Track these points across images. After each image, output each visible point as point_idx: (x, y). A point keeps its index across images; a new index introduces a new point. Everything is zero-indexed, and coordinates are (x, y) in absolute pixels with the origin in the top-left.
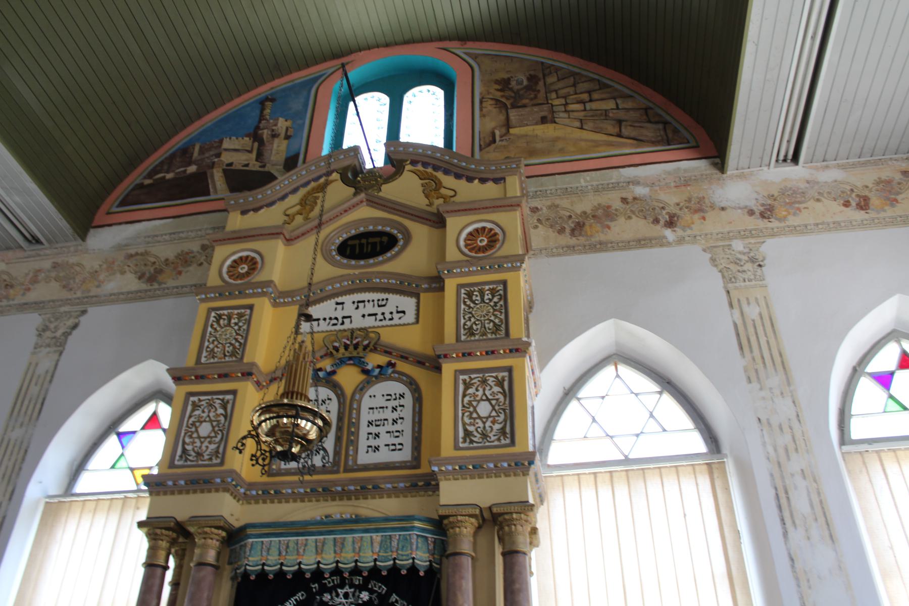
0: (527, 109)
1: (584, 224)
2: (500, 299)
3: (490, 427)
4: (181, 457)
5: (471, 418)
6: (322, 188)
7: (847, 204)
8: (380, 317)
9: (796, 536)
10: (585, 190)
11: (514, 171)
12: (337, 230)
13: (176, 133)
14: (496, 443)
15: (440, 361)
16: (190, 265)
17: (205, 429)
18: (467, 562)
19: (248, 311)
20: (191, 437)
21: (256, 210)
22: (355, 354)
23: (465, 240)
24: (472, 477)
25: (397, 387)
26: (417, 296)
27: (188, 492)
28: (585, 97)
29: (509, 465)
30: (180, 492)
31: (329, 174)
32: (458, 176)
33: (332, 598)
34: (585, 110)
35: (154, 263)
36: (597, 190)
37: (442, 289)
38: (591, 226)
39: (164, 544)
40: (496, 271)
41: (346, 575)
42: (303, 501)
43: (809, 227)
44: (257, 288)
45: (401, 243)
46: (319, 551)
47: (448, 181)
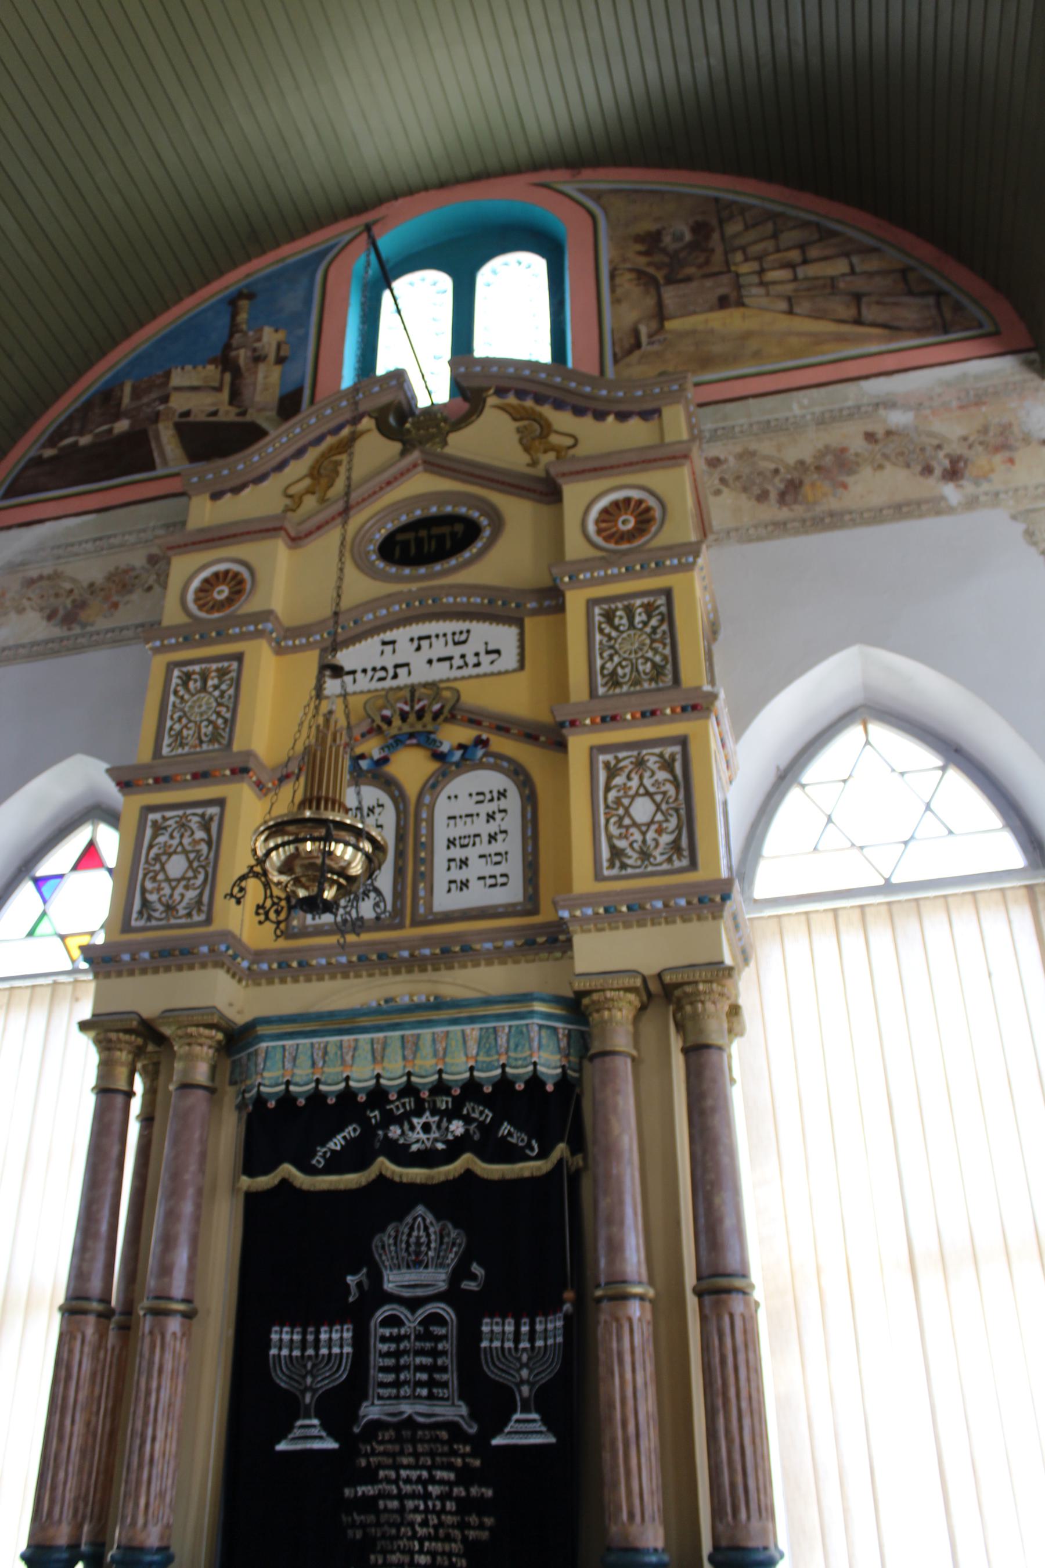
0: (694, 285)
1: (801, 483)
2: (662, 621)
3: (655, 840)
4: (140, 913)
5: (620, 826)
6: (347, 446)
8: (457, 662)
10: (801, 422)
11: (675, 397)
12: (374, 518)
13: (91, 364)
14: (665, 867)
15: (565, 731)
16: (130, 592)
17: (176, 866)
18: (624, 1067)
19: (235, 665)
20: (154, 879)
21: (236, 490)
22: (419, 727)
23: (597, 522)
24: (627, 925)
25: (492, 780)
26: (519, 623)
27: (156, 971)
28: (795, 255)
29: (689, 903)
30: (144, 971)
31: (356, 420)
32: (579, 411)
33: (403, 1133)
34: (795, 279)
35: (71, 591)
36: (822, 422)
37: (560, 608)
38: (813, 485)
39: (123, 1056)
40: (654, 573)
41: (425, 1094)
42: (345, 976)
44: (247, 624)
45: (487, 533)
46: (378, 1056)
47: (562, 420)
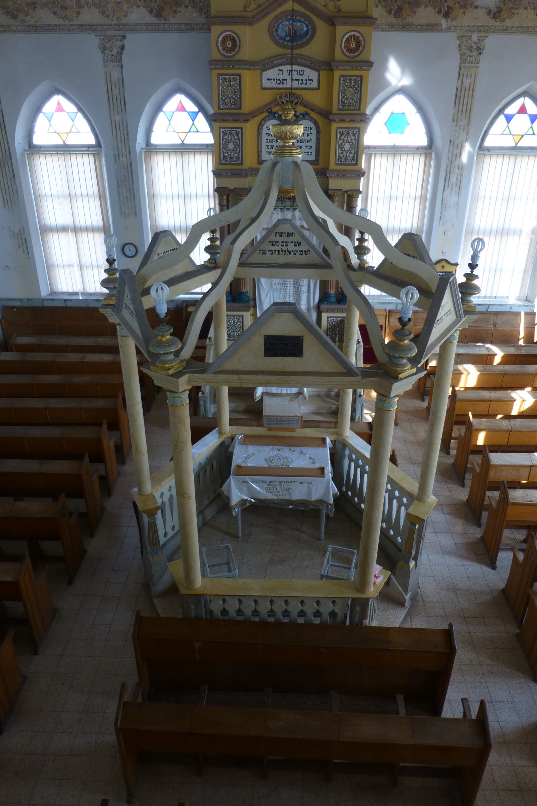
4: (223, 159)
9: (447, 191)
14: (350, 163)
16: (180, 6)
17: (231, 146)
20: (225, 149)
43: (513, 29)
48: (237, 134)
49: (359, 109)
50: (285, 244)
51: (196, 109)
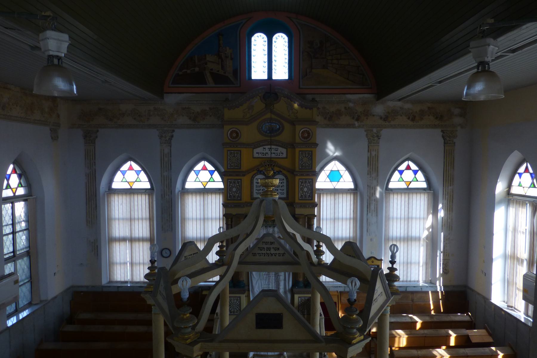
7: (409, 118)
9: (370, 214)
17: (234, 189)
48: (238, 183)
49: (312, 169)
50: (269, 249)
51: (214, 169)
